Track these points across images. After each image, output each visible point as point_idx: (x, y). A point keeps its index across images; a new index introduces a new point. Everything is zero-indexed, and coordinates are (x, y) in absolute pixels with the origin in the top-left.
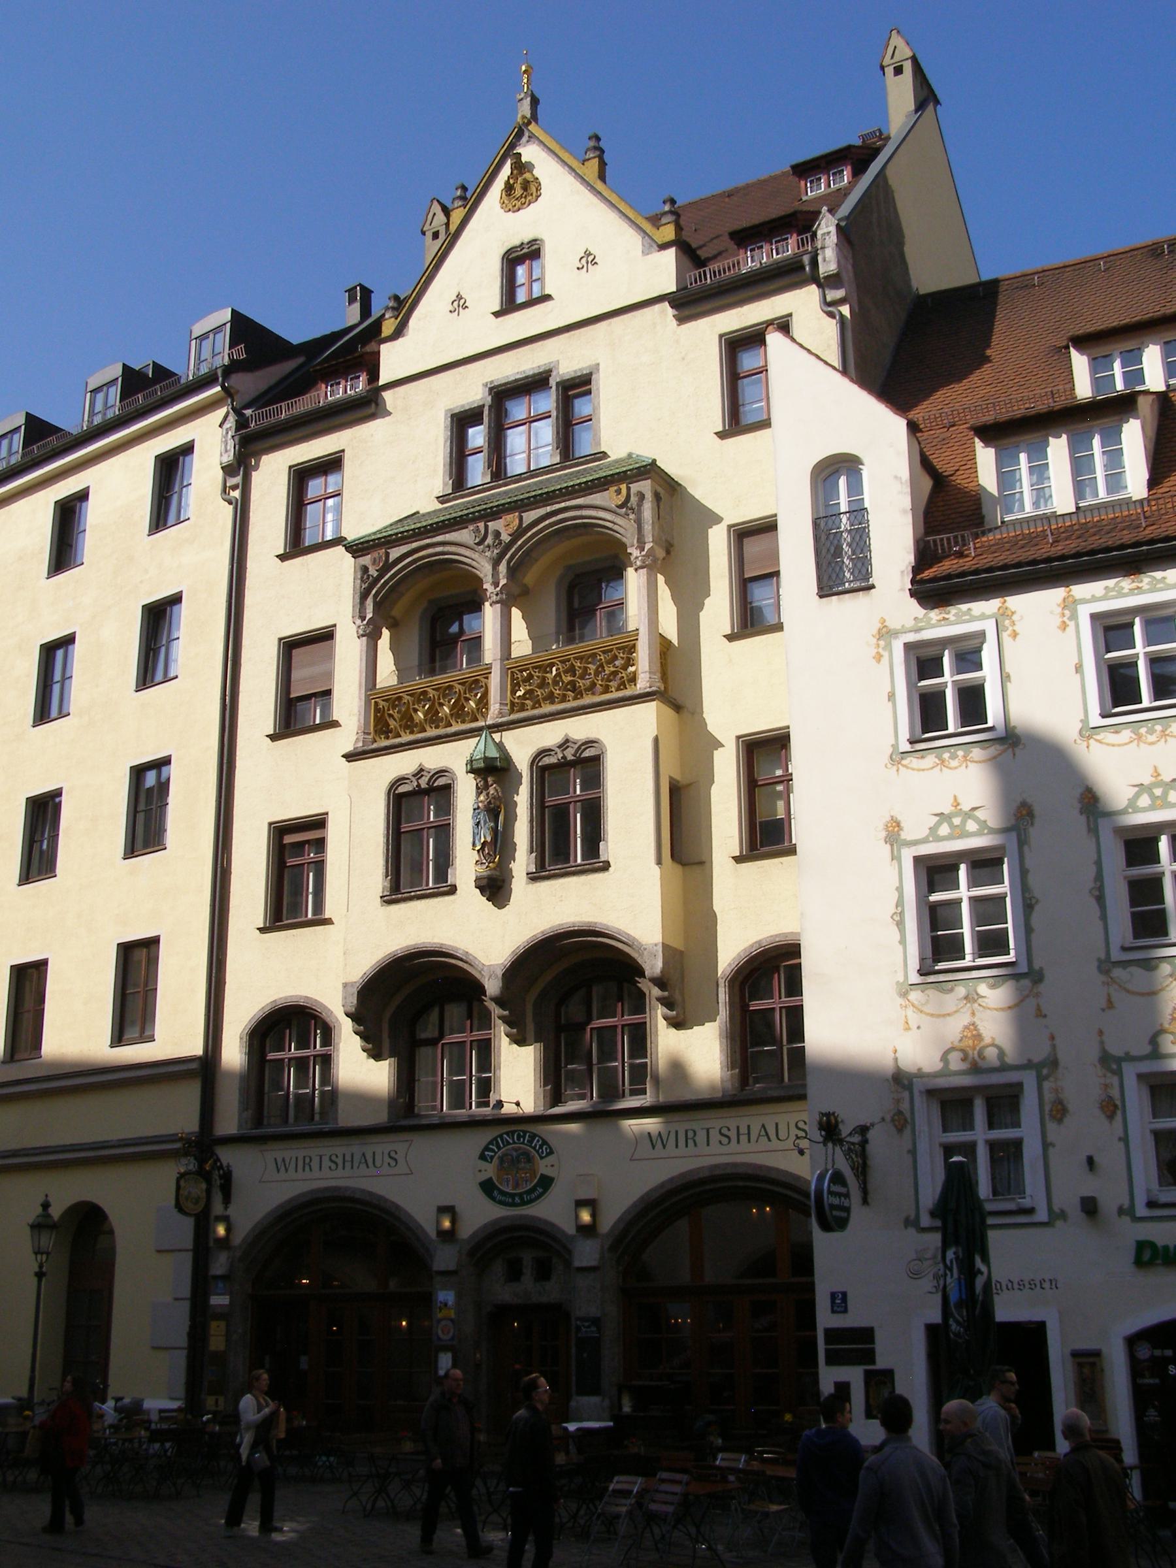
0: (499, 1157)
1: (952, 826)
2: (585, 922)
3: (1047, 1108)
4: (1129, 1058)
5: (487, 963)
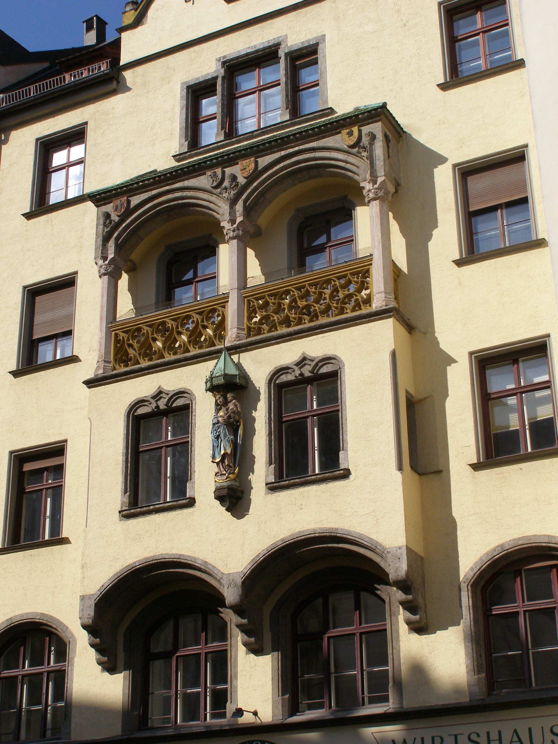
2: (326, 529)
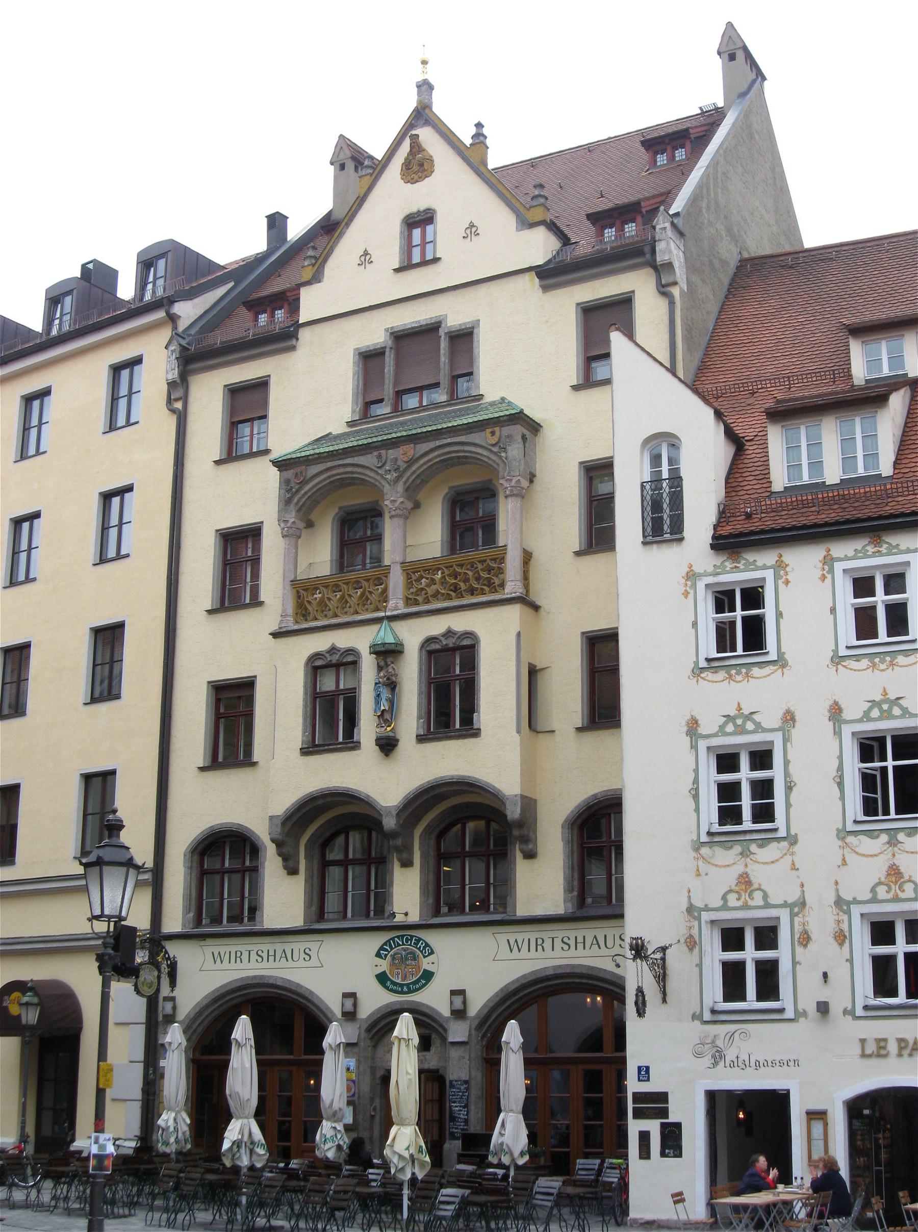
0: (391, 955)
1: (735, 725)
3: (797, 936)
4: (855, 901)
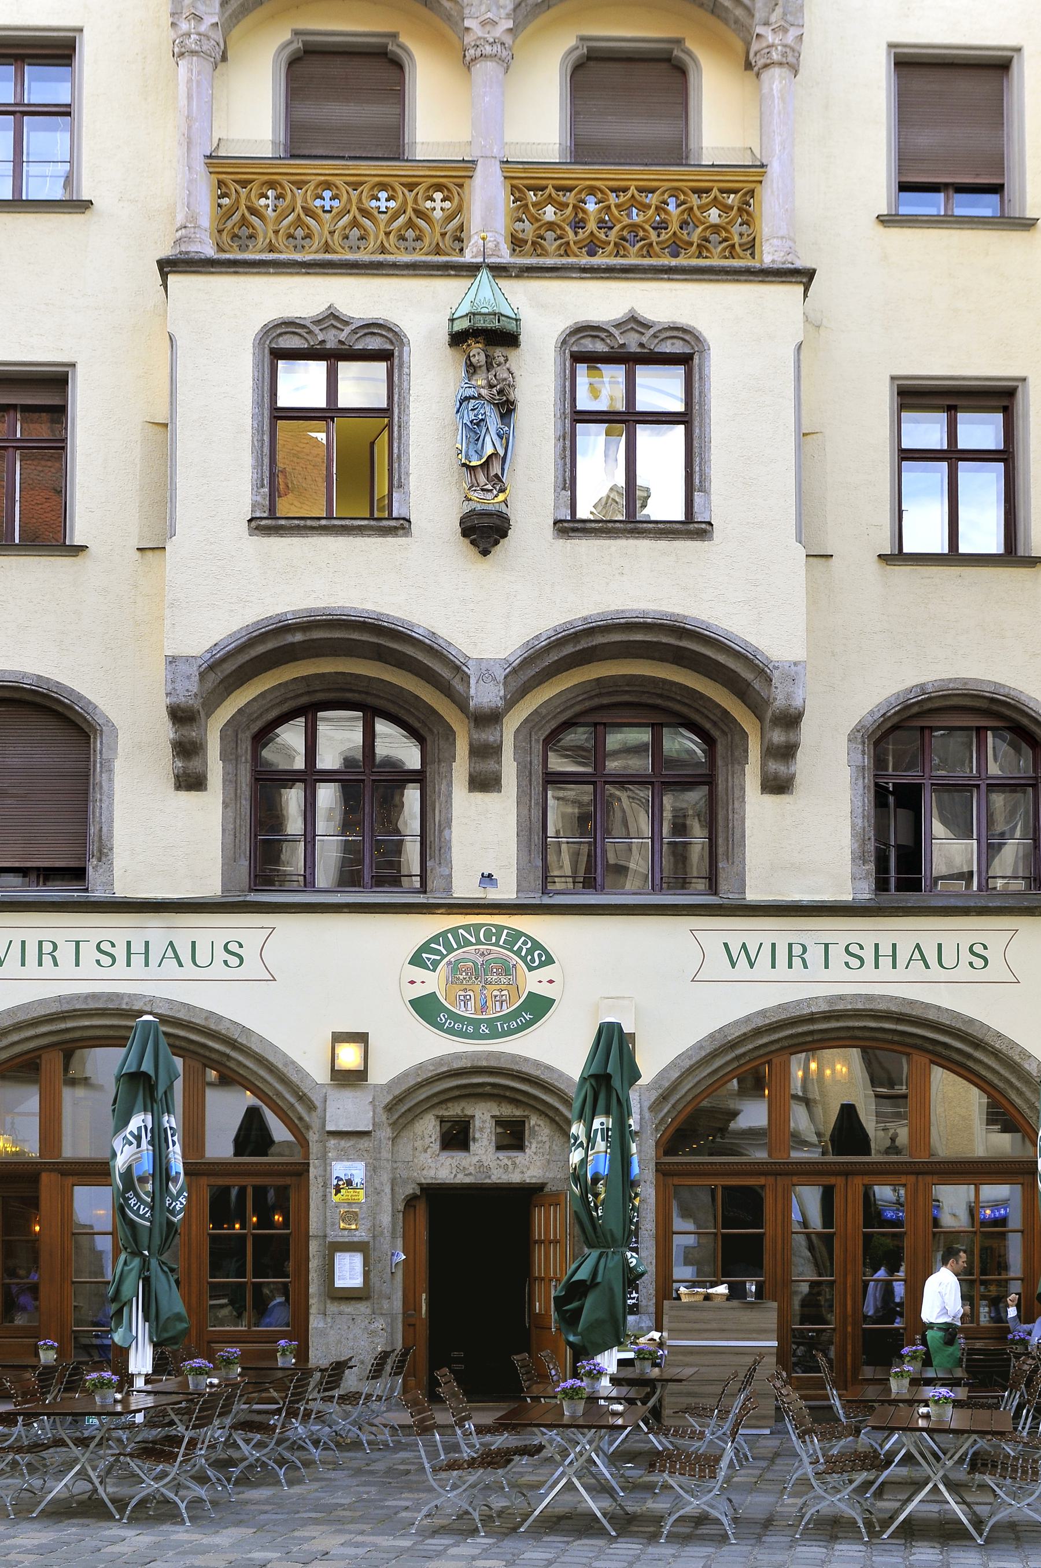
0: (449, 963)
2: (666, 614)
5: (474, 656)
